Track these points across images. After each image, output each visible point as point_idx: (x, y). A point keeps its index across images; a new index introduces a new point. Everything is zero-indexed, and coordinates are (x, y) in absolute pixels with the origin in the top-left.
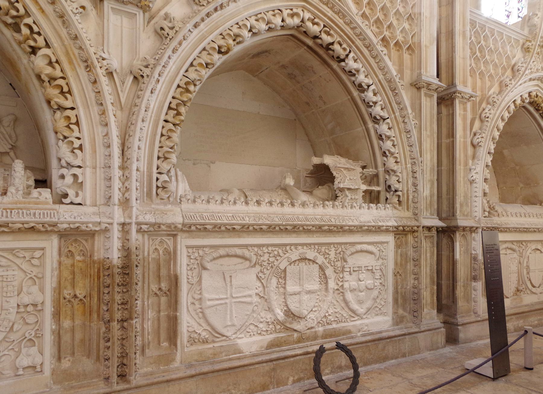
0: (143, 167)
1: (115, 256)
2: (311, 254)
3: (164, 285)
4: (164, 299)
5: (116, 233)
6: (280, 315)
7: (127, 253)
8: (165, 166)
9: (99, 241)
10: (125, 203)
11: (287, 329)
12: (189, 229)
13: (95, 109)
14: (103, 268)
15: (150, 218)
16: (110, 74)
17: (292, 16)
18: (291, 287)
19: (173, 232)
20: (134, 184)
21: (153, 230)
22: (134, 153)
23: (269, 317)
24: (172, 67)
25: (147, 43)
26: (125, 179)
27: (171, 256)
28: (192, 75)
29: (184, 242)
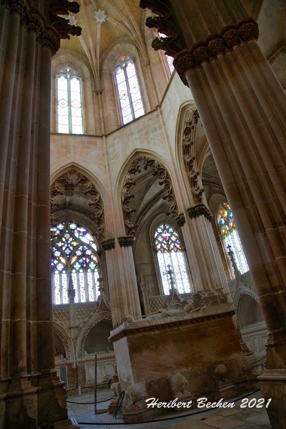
0: (78, 352)
1: (75, 367)
2: (110, 363)
3: (83, 371)
4: (83, 374)
5: (75, 363)
6: (105, 375)
7: (76, 366)
8: (82, 351)
9: (73, 365)
10: (76, 359)
11: (107, 378)
12: (87, 361)
13: (71, 345)
14: (73, 369)
15: (80, 360)
16: (72, 339)
17: (102, 318)
18: (107, 370)
19: (84, 362)
20: (77, 355)
21: (80, 362)
22: (77, 350)
23: (103, 376)
24: (81, 335)
25: (77, 332)
26: (75, 355)
27: (84, 366)
28: (85, 335)
29: (85, 363)
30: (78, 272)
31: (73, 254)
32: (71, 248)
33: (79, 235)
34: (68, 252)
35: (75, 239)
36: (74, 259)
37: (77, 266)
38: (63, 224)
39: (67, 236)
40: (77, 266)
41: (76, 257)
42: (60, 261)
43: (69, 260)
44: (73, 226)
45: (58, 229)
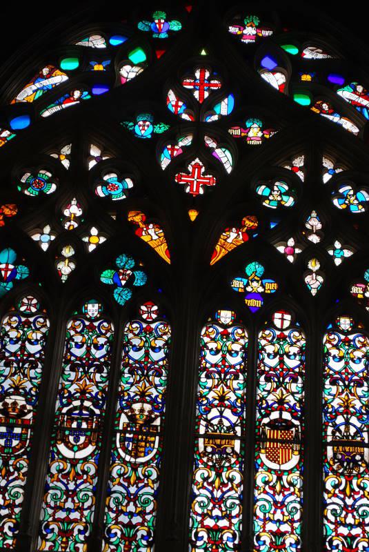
32: (225, 158)
34: (196, 181)
40: (254, 282)
43: (191, 241)
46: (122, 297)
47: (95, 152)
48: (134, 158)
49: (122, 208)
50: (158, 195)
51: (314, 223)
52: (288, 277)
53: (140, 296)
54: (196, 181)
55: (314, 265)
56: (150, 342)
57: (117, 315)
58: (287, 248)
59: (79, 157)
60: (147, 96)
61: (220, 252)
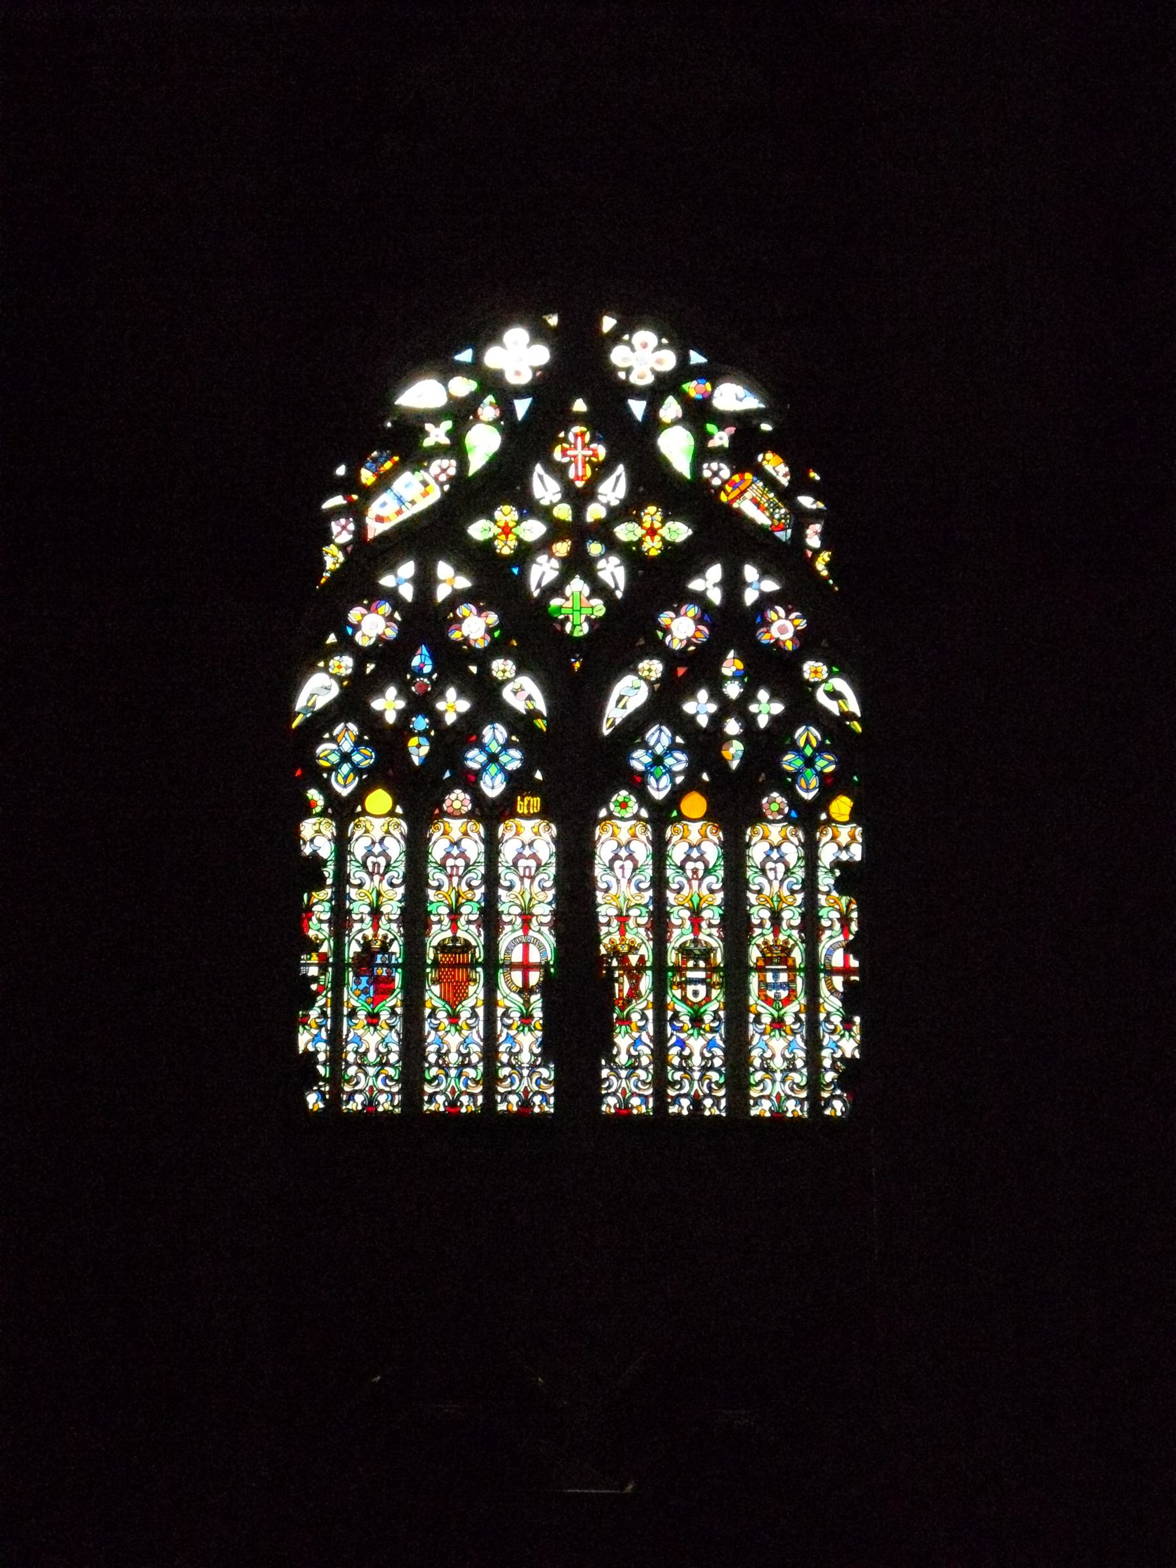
30: (662, 817)
31: (626, 631)
33: (703, 453)
35: (654, 484)
36: (628, 694)
37: (661, 757)
38: (539, 333)
39: (578, 449)
40: (661, 757)
41: (653, 668)
42: (487, 700)
44: (642, 356)
45: (491, 383)
46: (493, 786)
47: (444, 570)
48: (497, 578)
49: (484, 658)
50: (528, 630)
51: (731, 665)
52: (703, 744)
53: (518, 783)
54: (578, 609)
55: (732, 727)
56: (531, 839)
57: (491, 814)
58: (700, 707)
59: (425, 581)
60: (505, 482)
61: (614, 713)
